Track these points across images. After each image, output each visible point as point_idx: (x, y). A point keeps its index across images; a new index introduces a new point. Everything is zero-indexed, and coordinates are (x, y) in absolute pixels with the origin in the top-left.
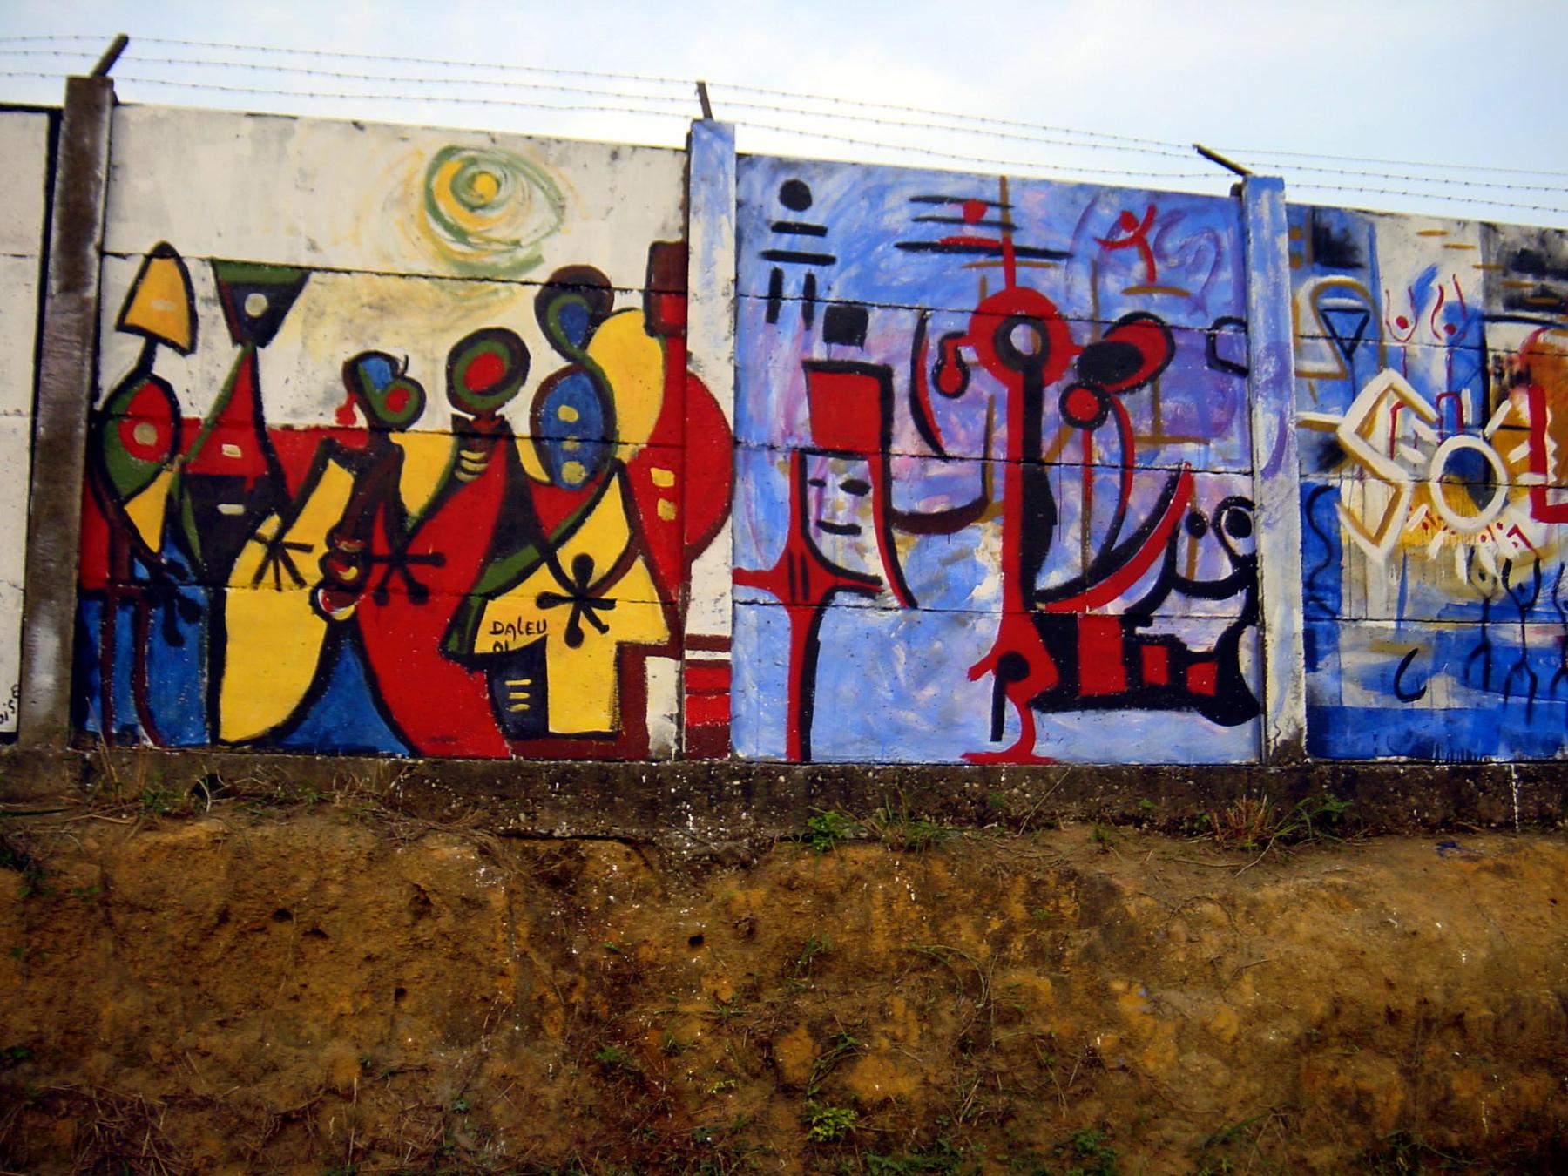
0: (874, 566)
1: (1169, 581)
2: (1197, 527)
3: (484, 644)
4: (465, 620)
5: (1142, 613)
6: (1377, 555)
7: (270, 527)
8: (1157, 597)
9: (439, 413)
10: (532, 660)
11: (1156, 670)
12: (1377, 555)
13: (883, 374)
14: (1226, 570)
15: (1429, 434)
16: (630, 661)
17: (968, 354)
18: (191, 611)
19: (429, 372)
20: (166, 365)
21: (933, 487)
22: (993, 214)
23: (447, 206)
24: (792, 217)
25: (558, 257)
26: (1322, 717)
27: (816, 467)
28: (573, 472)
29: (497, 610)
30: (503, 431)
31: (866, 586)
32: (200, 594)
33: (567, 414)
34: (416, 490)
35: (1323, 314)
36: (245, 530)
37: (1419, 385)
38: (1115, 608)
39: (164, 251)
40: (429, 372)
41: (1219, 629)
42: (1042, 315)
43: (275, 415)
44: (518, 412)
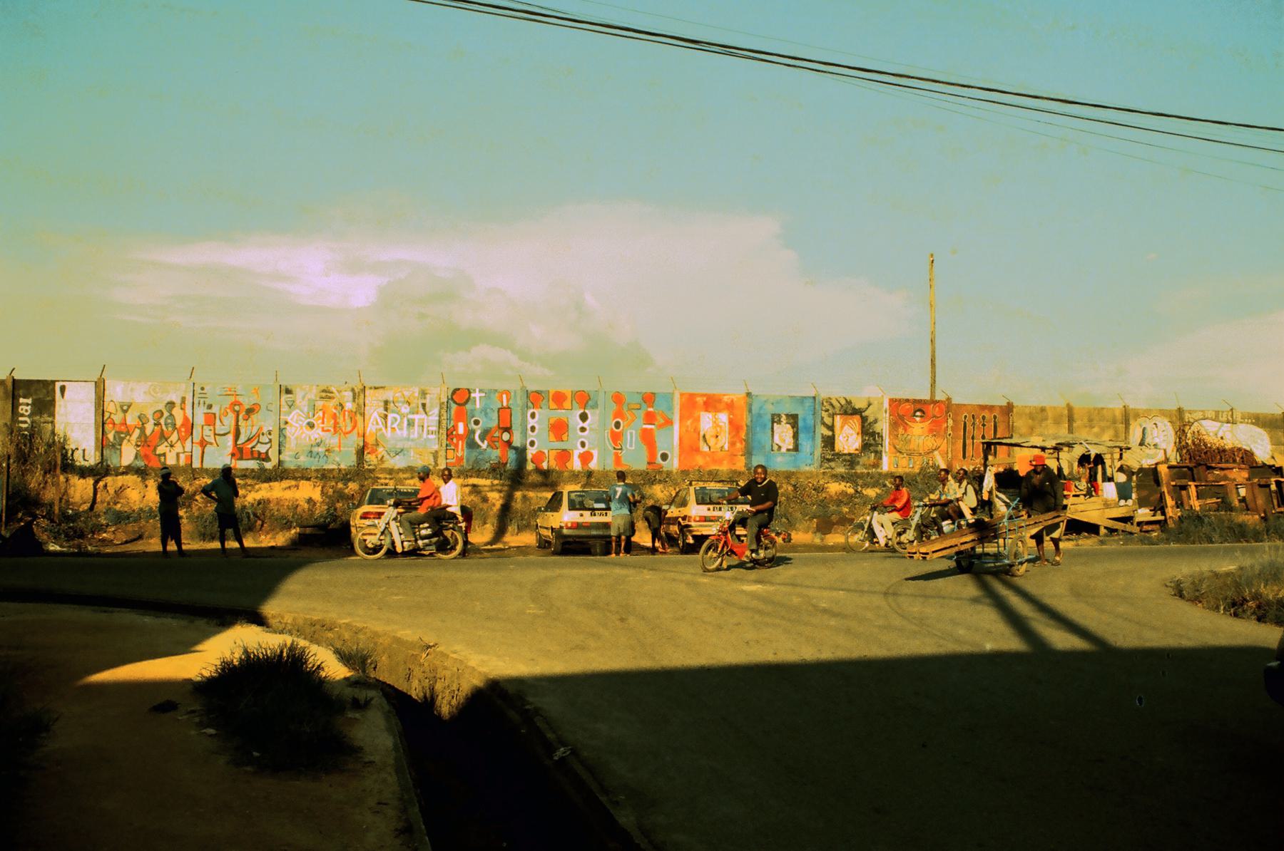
0: (213, 441)
1: (258, 442)
2: (263, 434)
3: (158, 453)
4: (155, 450)
5: (253, 447)
6: (293, 438)
7: (128, 437)
8: (257, 444)
9: (152, 422)
10: (164, 455)
11: (256, 456)
12: (293, 438)
13: (215, 414)
14: (267, 440)
15: (303, 419)
16: (178, 455)
17: (228, 410)
18: (117, 449)
19: (150, 415)
20: (112, 416)
21: (222, 430)
22: (233, 390)
23: (152, 393)
24: (202, 392)
25: (168, 399)
26: (280, 462)
27: (205, 427)
28: (170, 429)
29: (159, 448)
30: (160, 424)
31: (211, 444)
32: (119, 447)
33: (169, 421)
34: (148, 432)
35: (286, 402)
36: (123, 438)
37: (302, 412)
38: (250, 446)
39: (112, 401)
40: (150, 415)
41: (266, 449)
42: (240, 404)
43: (128, 423)
44: (162, 421)
